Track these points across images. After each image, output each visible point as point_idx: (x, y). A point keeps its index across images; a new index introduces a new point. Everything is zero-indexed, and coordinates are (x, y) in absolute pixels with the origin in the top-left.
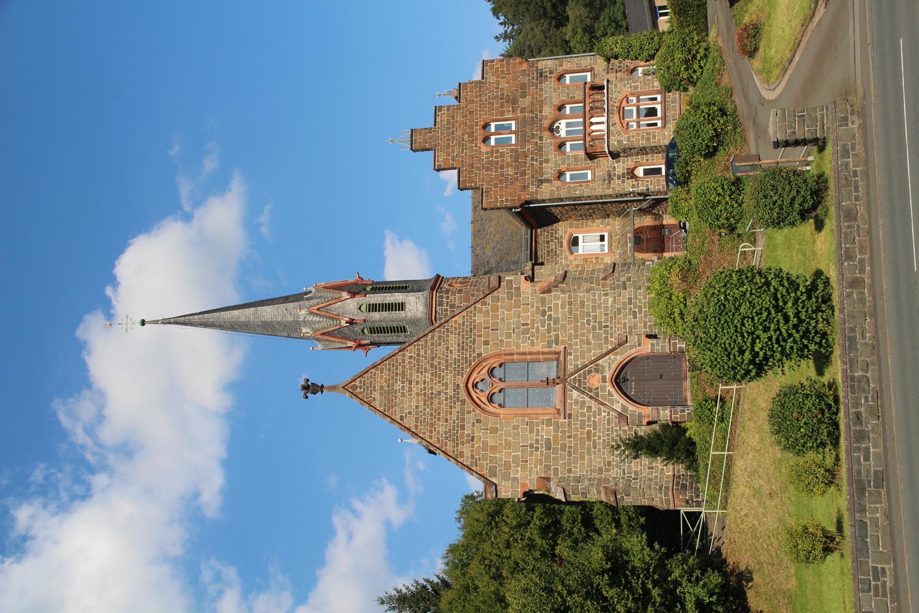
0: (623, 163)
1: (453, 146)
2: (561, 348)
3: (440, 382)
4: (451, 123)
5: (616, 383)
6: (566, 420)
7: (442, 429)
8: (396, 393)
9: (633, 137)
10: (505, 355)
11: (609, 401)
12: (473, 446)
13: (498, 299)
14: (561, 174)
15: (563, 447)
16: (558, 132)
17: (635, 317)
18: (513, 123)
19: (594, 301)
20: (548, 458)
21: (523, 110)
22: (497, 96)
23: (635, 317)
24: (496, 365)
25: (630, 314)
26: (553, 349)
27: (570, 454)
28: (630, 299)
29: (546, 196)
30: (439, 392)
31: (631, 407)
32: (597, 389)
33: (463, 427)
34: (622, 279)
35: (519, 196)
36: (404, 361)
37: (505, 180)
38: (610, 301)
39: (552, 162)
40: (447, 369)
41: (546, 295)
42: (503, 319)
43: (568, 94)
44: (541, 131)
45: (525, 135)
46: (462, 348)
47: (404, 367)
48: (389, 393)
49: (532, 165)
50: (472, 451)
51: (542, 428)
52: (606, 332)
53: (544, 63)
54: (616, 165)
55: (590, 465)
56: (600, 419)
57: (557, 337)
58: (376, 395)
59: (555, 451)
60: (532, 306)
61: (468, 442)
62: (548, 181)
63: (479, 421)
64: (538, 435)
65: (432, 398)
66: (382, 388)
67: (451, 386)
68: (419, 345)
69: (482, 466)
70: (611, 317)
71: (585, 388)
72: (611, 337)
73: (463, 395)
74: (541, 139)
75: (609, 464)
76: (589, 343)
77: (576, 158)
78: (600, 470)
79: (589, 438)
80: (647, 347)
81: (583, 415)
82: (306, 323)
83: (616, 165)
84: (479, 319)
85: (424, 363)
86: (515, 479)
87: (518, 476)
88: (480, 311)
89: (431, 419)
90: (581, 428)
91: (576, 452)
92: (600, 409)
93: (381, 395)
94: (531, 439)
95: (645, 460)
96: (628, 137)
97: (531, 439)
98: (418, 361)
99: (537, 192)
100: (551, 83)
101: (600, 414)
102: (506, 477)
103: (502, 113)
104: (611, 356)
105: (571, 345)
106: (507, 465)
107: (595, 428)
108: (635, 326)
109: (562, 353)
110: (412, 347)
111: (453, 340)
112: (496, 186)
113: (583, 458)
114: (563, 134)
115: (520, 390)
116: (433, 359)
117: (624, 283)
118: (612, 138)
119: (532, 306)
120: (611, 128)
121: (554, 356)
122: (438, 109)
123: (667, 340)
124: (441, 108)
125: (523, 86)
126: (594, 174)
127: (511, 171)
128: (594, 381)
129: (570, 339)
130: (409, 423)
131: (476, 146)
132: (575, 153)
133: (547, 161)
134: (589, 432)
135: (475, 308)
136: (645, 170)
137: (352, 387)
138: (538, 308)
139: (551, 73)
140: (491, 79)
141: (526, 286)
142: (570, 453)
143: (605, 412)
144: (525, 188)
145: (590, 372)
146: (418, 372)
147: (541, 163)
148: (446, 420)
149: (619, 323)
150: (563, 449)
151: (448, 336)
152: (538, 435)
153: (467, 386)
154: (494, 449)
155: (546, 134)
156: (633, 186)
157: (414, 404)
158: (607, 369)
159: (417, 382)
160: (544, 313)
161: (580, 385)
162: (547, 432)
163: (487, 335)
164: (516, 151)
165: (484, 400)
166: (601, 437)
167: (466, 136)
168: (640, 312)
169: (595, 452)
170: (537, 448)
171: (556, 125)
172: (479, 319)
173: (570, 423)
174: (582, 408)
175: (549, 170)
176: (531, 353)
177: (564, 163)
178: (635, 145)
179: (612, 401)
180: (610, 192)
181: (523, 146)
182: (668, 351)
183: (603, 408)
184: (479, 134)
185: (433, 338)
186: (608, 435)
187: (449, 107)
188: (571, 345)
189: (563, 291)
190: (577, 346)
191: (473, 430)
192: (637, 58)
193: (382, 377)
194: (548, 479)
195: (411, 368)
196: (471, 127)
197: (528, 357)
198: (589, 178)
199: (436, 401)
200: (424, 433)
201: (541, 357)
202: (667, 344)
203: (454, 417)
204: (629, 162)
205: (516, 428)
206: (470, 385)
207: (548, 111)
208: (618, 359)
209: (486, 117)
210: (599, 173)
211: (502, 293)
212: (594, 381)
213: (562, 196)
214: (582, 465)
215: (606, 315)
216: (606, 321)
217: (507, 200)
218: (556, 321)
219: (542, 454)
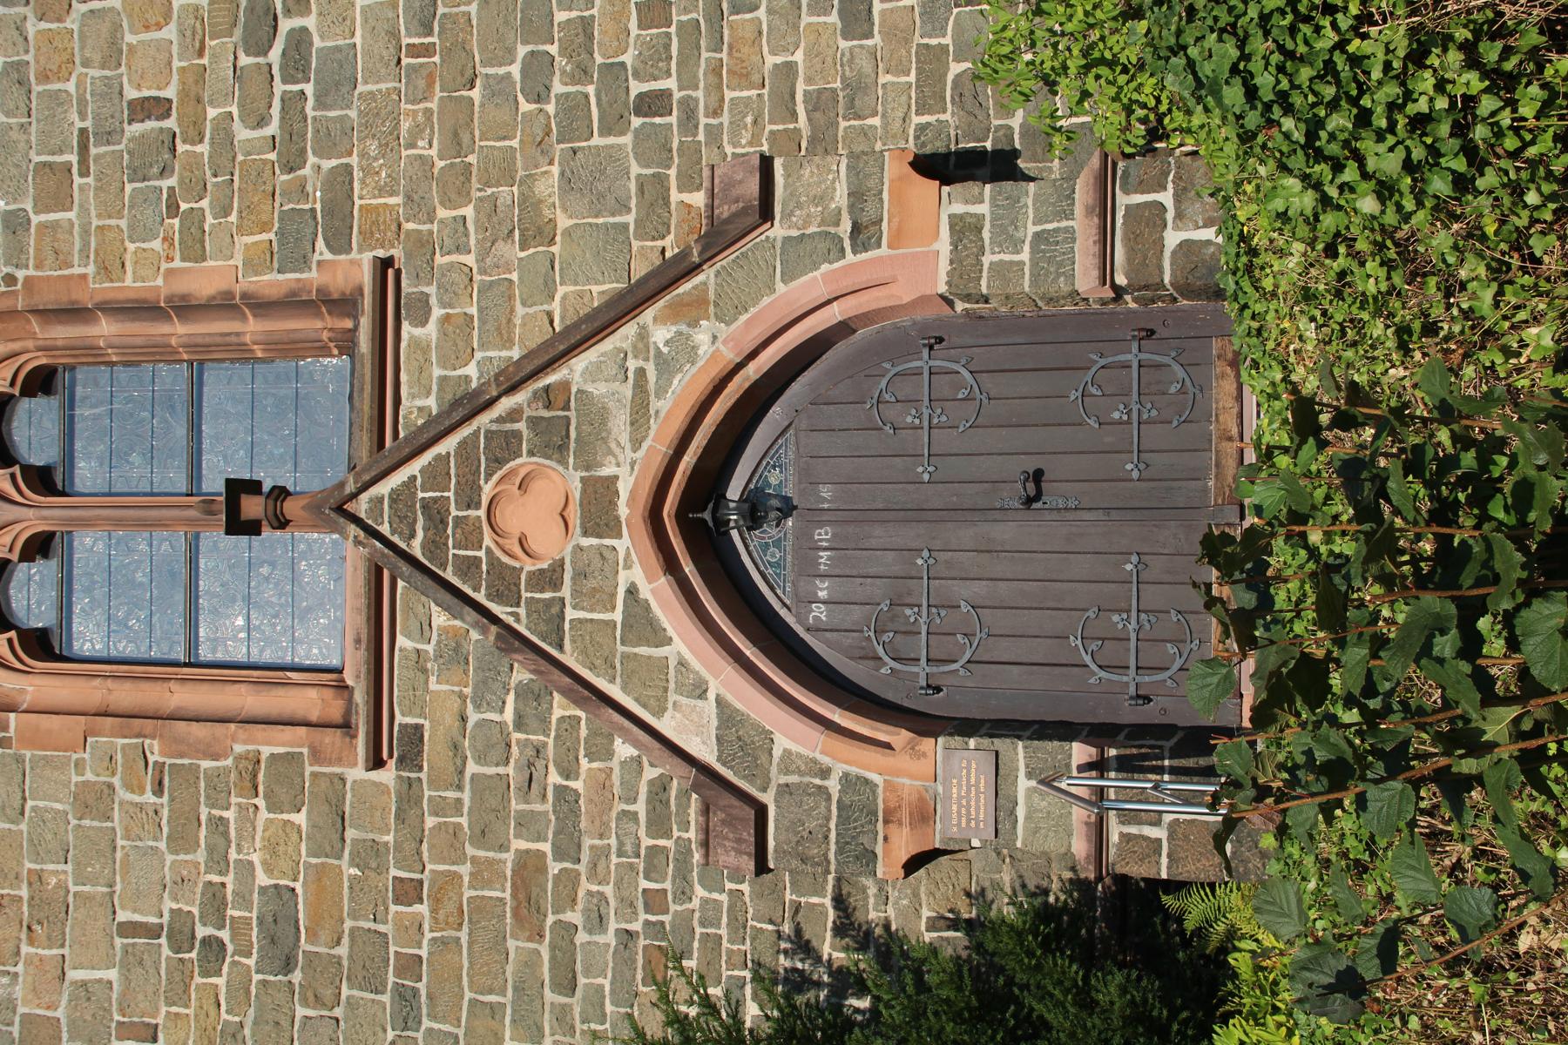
2: (357, 267)
6: (387, 776)
11: (635, 672)
26: (312, 275)
32: (550, 578)
51: (248, 815)
52: (655, 148)
64: (219, 861)
70: (690, 32)
71: (468, 567)
72: (687, 184)
76: (538, 232)
80: (923, 252)
81: (496, 745)
90: (482, 836)
104: (656, 327)
105: (424, 245)
107: (568, 848)
108: (858, 88)
123: (1083, 191)
128: (534, 514)
129: (418, 205)
142: (406, 998)
145: (503, 446)
149: (743, 77)
152: (219, 861)
161: (435, 546)
162: (272, 848)
169: (562, 1018)
170: (214, 949)
173: (409, 795)
176: (185, 308)
179: (651, 678)
186: (654, 901)
197: (178, 331)
201: (252, 328)
202: (1082, 225)
208: (696, 348)
216: (654, 61)
218: (337, 83)
219: (240, 989)
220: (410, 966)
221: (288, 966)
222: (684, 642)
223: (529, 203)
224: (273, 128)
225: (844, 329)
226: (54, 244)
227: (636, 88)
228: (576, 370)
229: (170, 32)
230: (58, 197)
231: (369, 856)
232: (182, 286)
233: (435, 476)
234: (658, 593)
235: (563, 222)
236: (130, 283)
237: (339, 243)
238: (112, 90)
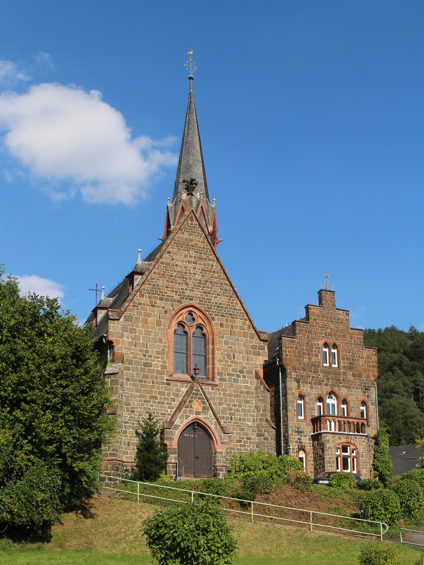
0: (309, 443)
1: (323, 320)
2: (217, 382)
3: (195, 285)
4: (338, 321)
5: (193, 423)
6: (165, 381)
7: (160, 282)
8: (188, 250)
9: (331, 451)
10: (213, 339)
12: (148, 305)
13: (252, 338)
14: (301, 397)
16: (329, 398)
17: (238, 441)
18: (336, 366)
19: (249, 411)
20: (138, 363)
21: (344, 374)
22: (354, 356)
23: (238, 441)
24: (205, 331)
25: (240, 437)
27: (140, 381)
28: (250, 439)
29: (288, 384)
30: (187, 284)
31: (178, 433)
32: (191, 407)
33: (161, 299)
34: (266, 434)
35: (289, 365)
36: (210, 260)
37: (301, 355)
38: (249, 423)
39: (312, 392)
40: (204, 292)
41: (254, 374)
42: (238, 340)
43: (354, 407)
44: (331, 385)
45: (329, 373)
46: (219, 306)
47: (206, 259)
49: (309, 377)
50: (144, 304)
51: (160, 361)
52: (227, 418)
53: (374, 392)
54: (307, 437)
55: (132, 396)
56: (165, 408)
57: (224, 380)
58: (186, 236)
59: (142, 370)
60: (247, 364)
61: (151, 302)
62: (299, 387)
63: (166, 312)
64: (155, 357)
65: (183, 278)
66: (191, 240)
67: (191, 294)
68: (221, 273)
69: (133, 310)
70: (238, 423)
74: (326, 385)
75: (133, 412)
77: (313, 409)
78: (128, 404)
79: (152, 397)
80: (220, 448)
81: (169, 395)
83: (307, 437)
84: (239, 322)
85: (208, 275)
86: (122, 336)
87: (125, 339)
88: (244, 324)
89: (168, 275)
91: (142, 386)
92: (172, 408)
93: (186, 239)
94: (152, 351)
95: (136, 440)
96: (331, 448)
97: (152, 352)
98: (210, 271)
99: (292, 378)
101: (169, 408)
102: (124, 329)
103: (343, 359)
104: (214, 421)
105: (219, 390)
106: (133, 331)
107: (159, 403)
109: (214, 383)
110: (219, 268)
111: (224, 300)
112: (297, 348)
113: (137, 391)
114: (328, 401)
115: (185, 347)
116: (211, 282)
117: (262, 435)
118: (331, 436)
119: (247, 364)
120: (337, 436)
121: (210, 376)
122: (347, 312)
123: (225, 464)
124: (348, 315)
125: (360, 376)
126: (302, 421)
127: (306, 360)
128: (197, 406)
129: (223, 390)
130: (166, 258)
131: (323, 337)
132: (316, 409)
133: (311, 388)
135: (246, 320)
136: (303, 458)
137: (192, 217)
138: (245, 367)
143: (171, 412)
144: (294, 369)
145: (204, 403)
146: (202, 270)
147: (310, 383)
148: (167, 287)
149: (233, 429)
150: (145, 376)
151: (227, 296)
152: (155, 357)
154: (145, 321)
155: (329, 389)
156: (293, 449)
157: (179, 263)
158: (205, 416)
159: (195, 268)
160: (241, 372)
162: (157, 364)
163: (227, 327)
164: (319, 366)
165: (180, 319)
166: (153, 407)
167: (330, 331)
168: (241, 446)
170: (145, 356)
171: (334, 397)
172: (239, 322)
173: (163, 383)
174: (174, 394)
176: (213, 358)
177: (310, 399)
178: (326, 452)
180: (290, 432)
181: (322, 371)
182: (218, 464)
183: (173, 410)
184: (330, 341)
185: (226, 285)
187: (348, 320)
188: (219, 390)
189: (257, 388)
191: (159, 307)
192: (375, 458)
193: (199, 241)
194: (123, 362)
195: (205, 265)
196: (335, 335)
198: (300, 418)
199: (181, 280)
200: (158, 268)
202: (222, 464)
203: (169, 293)
204: (309, 448)
205: (161, 341)
206: (191, 309)
207: (343, 392)
208: (212, 425)
209: (341, 347)
210: (303, 425)
211: (256, 341)
212: (197, 406)
213: (288, 396)
214: (132, 390)
215: (240, 419)
216: (236, 419)
217: (287, 355)
219: (141, 359)
220: (145, 382)
221: (144, 366)
223: (223, 404)
224: (231, 372)
225: (212, 439)
226: (220, 342)
227: (233, 417)
228: (210, 411)
229: (241, 360)
231: (157, 378)
232: (216, 359)
233: (200, 394)
234: (190, 419)
235: (221, 407)
236: (216, 352)
237: (220, 380)
238: (236, 352)
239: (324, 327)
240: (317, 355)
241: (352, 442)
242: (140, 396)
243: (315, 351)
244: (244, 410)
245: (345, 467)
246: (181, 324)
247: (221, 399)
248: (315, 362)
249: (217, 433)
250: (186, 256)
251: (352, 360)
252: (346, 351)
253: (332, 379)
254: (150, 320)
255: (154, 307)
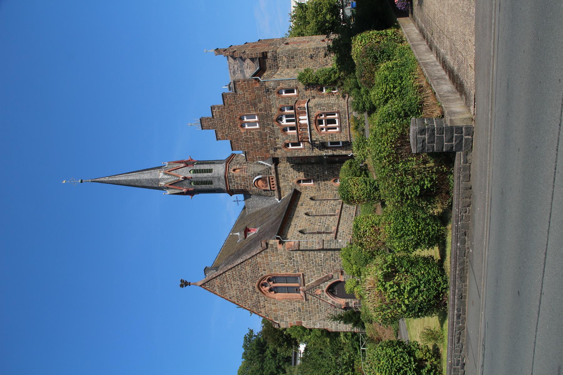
2: (301, 273)
15: (306, 311)
20: (300, 315)
27: (310, 313)
30: (246, 289)
33: (259, 302)
45: (264, 124)
48: (222, 289)
60: (285, 255)
62: (280, 148)
66: (218, 286)
73: (257, 290)
74: (273, 126)
76: (314, 272)
82: (162, 179)
84: (259, 260)
85: (235, 277)
94: (292, 307)
98: (233, 276)
100: (274, 96)
106: (282, 317)
107: (320, 304)
111: (248, 268)
112: (252, 150)
113: (315, 314)
116: (240, 276)
127: (259, 143)
128: (319, 292)
133: (278, 138)
134: (317, 306)
139: (274, 89)
140: (240, 92)
141: (280, 247)
144: (268, 151)
145: (316, 288)
147: (275, 139)
153: (258, 286)
154: (275, 311)
155: (275, 123)
172: (259, 260)
175: (280, 143)
177: (287, 139)
181: (264, 130)
184: (239, 123)
187: (219, 107)
190: (308, 273)
203: (255, 298)
205: (285, 303)
207: (275, 111)
208: (329, 283)
212: (319, 292)
222: (329, 298)
230: (275, 268)
234: (327, 295)
239: (229, 127)
240: (253, 134)
241: (314, 119)
242: (318, 313)
243: (250, 135)
244: (315, 257)
245: (333, 121)
246: (271, 290)
247: (311, 271)
248: (258, 135)
249: (333, 281)
250: (229, 289)
251: (248, 103)
252: (243, 109)
253: (267, 121)
254: (273, 308)
255: (265, 307)
